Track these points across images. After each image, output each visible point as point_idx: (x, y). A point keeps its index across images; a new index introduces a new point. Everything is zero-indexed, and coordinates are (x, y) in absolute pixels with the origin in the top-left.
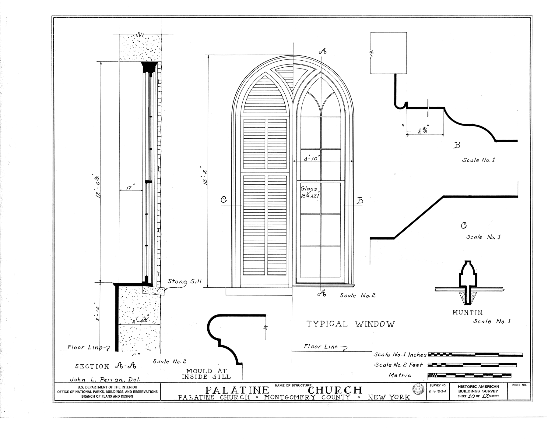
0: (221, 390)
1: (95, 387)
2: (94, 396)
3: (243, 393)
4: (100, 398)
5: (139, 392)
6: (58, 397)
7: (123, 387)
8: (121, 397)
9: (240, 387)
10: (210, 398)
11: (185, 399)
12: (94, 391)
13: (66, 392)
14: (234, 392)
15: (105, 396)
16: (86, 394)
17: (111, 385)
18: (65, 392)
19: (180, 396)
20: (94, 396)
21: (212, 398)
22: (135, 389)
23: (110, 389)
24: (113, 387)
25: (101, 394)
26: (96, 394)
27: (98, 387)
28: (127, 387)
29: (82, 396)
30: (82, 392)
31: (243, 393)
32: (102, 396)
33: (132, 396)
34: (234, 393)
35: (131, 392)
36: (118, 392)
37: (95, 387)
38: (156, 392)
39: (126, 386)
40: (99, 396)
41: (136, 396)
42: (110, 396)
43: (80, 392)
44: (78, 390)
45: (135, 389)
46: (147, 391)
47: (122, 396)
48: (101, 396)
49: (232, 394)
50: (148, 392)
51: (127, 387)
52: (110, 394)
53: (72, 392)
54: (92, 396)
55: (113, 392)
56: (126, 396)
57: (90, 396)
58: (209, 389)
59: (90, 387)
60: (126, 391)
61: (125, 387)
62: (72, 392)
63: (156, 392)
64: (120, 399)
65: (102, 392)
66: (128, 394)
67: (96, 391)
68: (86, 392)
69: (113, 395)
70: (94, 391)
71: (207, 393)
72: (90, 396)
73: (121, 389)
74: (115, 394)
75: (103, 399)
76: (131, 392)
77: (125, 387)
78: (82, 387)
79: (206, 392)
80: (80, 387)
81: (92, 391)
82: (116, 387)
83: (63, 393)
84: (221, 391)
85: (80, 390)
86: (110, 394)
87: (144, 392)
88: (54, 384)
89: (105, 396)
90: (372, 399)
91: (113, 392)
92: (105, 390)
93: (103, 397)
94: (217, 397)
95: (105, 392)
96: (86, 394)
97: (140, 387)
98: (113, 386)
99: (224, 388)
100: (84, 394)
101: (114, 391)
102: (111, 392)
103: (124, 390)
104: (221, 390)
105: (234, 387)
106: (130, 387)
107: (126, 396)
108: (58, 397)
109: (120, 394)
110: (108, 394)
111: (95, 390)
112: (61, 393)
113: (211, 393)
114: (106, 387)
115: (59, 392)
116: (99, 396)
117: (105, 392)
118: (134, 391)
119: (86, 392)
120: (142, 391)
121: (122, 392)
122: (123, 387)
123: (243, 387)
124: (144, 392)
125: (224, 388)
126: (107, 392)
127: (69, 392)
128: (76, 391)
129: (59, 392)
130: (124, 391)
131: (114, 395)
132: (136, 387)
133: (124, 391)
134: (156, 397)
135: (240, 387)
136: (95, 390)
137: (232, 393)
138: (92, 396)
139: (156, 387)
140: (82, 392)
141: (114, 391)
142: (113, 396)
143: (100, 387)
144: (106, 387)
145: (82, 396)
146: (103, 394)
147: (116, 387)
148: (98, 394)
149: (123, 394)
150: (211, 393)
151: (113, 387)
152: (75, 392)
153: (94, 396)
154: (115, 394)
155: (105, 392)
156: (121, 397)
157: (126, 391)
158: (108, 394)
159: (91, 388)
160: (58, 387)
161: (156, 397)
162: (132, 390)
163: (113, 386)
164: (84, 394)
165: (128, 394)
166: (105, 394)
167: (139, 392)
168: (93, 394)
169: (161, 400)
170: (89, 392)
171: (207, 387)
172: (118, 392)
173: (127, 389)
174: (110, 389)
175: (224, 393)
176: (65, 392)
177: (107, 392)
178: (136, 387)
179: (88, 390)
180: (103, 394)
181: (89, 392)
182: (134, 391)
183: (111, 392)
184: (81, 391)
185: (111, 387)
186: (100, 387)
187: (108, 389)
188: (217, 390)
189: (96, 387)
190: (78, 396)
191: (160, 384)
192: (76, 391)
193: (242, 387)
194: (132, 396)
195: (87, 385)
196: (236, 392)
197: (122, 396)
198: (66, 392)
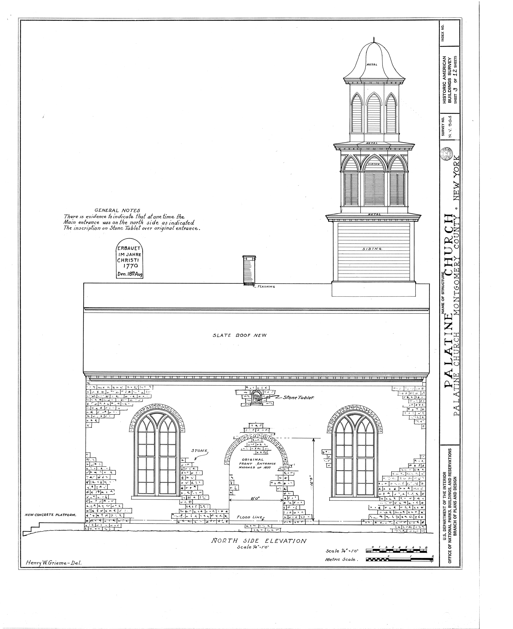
0: (448, 368)
1: (444, 521)
2: (455, 521)
3: (451, 342)
4: (457, 514)
5: (450, 469)
6: (455, 562)
7: (444, 488)
8: (456, 490)
9: (445, 345)
10: (457, 377)
11: (458, 408)
12: (449, 522)
13: (450, 553)
14: (451, 353)
15: (455, 509)
16: (452, 531)
17: (442, 502)
18: (450, 555)
19: (455, 414)
20: (455, 522)
21: (457, 375)
22: (447, 474)
23: (447, 502)
24: (445, 499)
25: (452, 513)
26: (453, 519)
27: (444, 517)
28: (444, 484)
29: (455, 535)
30: (449, 535)
31: (451, 342)
32: (454, 512)
33: (455, 478)
34: (451, 351)
35: (450, 479)
36: (450, 494)
37: (444, 521)
38: (450, 450)
39: (443, 484)
40: (455, 516)
41: (455, 473)
42: (455, 503)
43: (450, 537)
44: (447, 540)
45: (447, 474)
46: (449, 461)
47: (455, 488)
48: (455, 513)
49: (453, 354)
50: (450, 460)
51: (444, 484)
52: (452, 503)
53: (450, 546)
54: (455, 524)
55: (450, 500)
56: (455, 484)
57: (455, 526)
58: (447, 384)
59: (444, 525)
60: (449, 484)
61: (444, 485)
62: (450, 546)
63: (450, 451)
64: (458, 491)
65: (450, 513)
66: (452, 482)
67: (449, 519)
68: (450, 530)
69: (453, 500)
70: (449, 522)
71: (451, 386)
72: (455, 526)
73: (447, 490)
74: (452, 497)
75: (458, 511)
76: (450, 479)
77: (444, 485)
78: (445, 535)
79: (451, 387)
80: (444, 537)
81: (449, 524)
82: (444, 496)
83: (451, 557)
84: (449, 367)
85: (447, 538)
86: (452, 503)
87: (450, 465)
88: (440, 567)
89: (455, 509)
90: (459, 312)
91: (450, 500)
92: (448, 509)
93: (456, 511)
94: (456, 370)
95: (450, 508)
96: (452, 531)
97: (445, 468)
98: (443, 499)
99: (445, 364)
100: (452, 533)
101: (449, 499)
102: (450, 502)
103: (448, 486)
104: (448, 368)
105: (446, 351)
106: (444, 480)
107: (455, 484)
108: (455, 562)
109: (453, 491)
110: (452, 505)
111: (447, 520)
112: (451, 559)
113: (451, 381)
114: (444, 508)
115: (450, 561)
116: (455, 516)
117: (449, 509)
118: (450, 475)
119: (450, 530)
120: (449, 466)
121: (450, 489)
122: (444, 488)
123: (445, 342)
124: (450, 465)
125: (445, 364)
126: (450, 507)
127: (450, 550)
128: (449, 542)
129: (450, 561)
130: (449, 486)
131: (454, 498)
132: (444, 473)
133: (449, 486)
134: (455, 450)
135: (445, 345)
136: (447, 520)
137: (451, 354)
138: (455, 524)
139: (444, 450)
140: (449, 535)
141: (449, 499)
142: (455, 500)
143: (445, 515)
144: (444, 508)
145: (455, 535)
146: (452, 511)
147: (444, 496)
148: (452, 516)
149: (452, 488)
150: (451, 381)
151: (445, 499)
152: (450, 543)
153: (455, 522)
154: (452, 497)
155: (449, 509)
156: (456, 490)
157: (449, 484)
158: (452, 505)
159: (445, 525)
160: (444, 562)
161: (455, 450)
162: (447, 477)
163: (443, 499)
164: (452, 533)
165: (452, 482)
166: (453, 508)
167: (450, 469)
168: (452, 523)
169: (460, 445)
170: (450, 527)
171: (446, 386)
172: (450, 494)
173: (447, 483)
174: (447, 502)
175: (451, 364)
176: (450, 555)
177: (450, 507)
178: (444, 473)
179: (447, 529)
180: (452, 511)
181: (450, 527)
182: (450, 475)
183: (450, 502)
184: (449, 536)
185: (444, 501)
186: (445, 515)
187: (447, 505)
188: (448, 373)
189: (445, 519)
190: (455, 539)
191: (440, 446)
192: (449, 542)
193: (446, 343)
194: (455, 478)
195: (442, 529)
196: (450, 349)
197: (455, 488)
198: (450, 553)
